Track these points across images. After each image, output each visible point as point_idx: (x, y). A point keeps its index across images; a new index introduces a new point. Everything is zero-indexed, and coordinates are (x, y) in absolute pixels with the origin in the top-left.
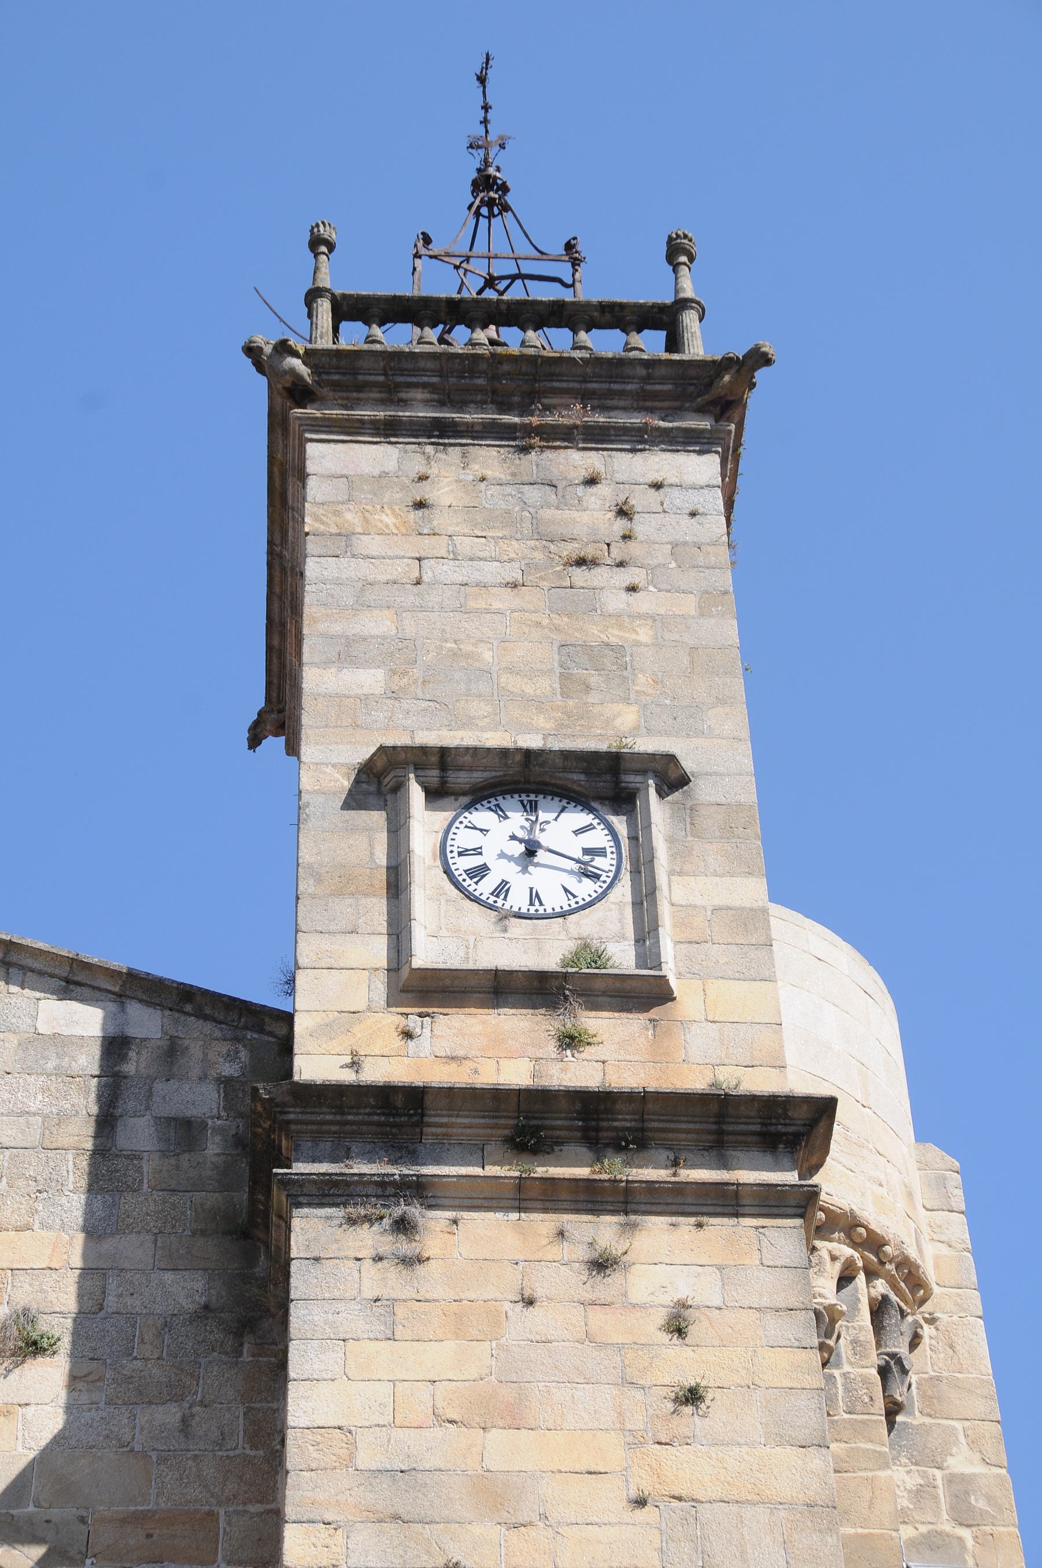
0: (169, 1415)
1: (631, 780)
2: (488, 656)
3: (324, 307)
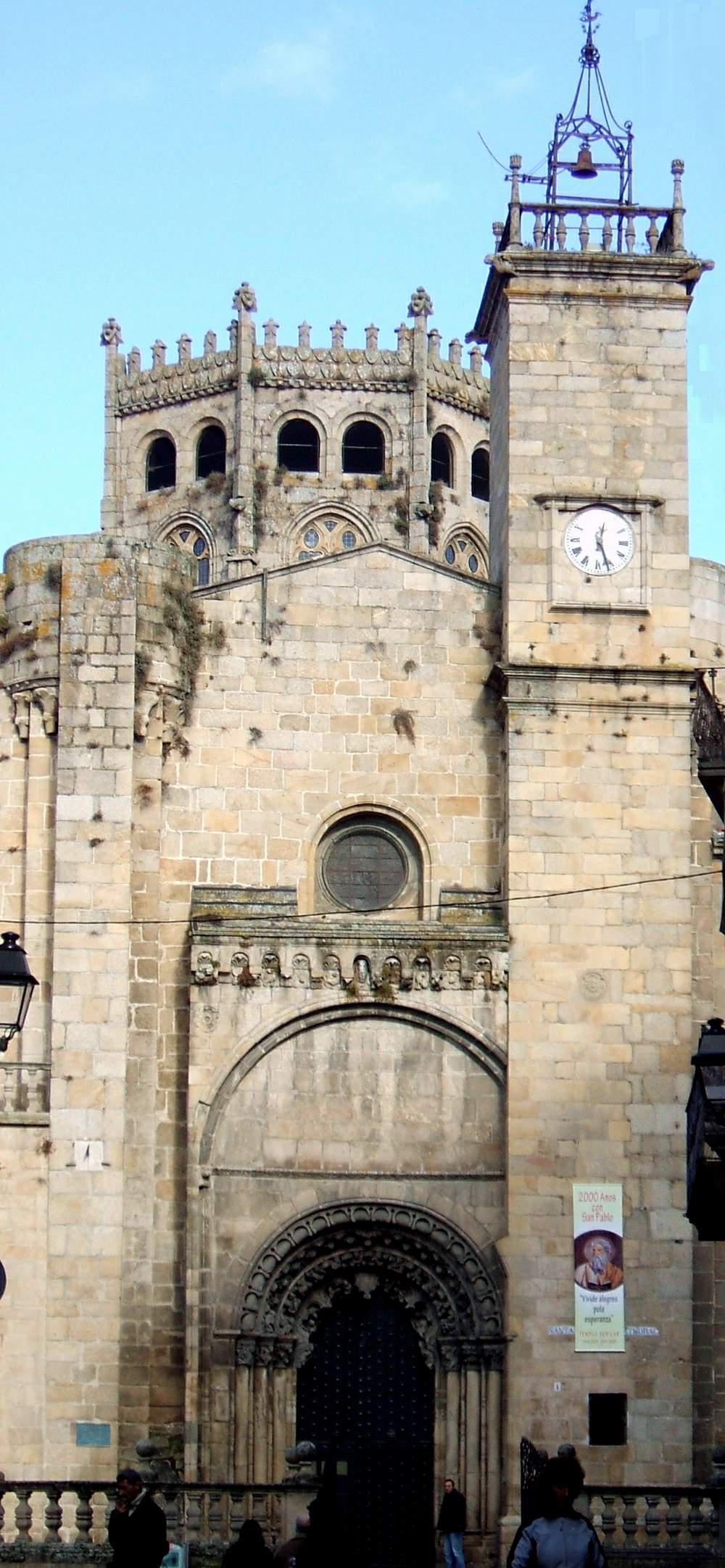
0: (461, 758)
1: (639, 507)
2: (584, 433)
3: (516, 210)
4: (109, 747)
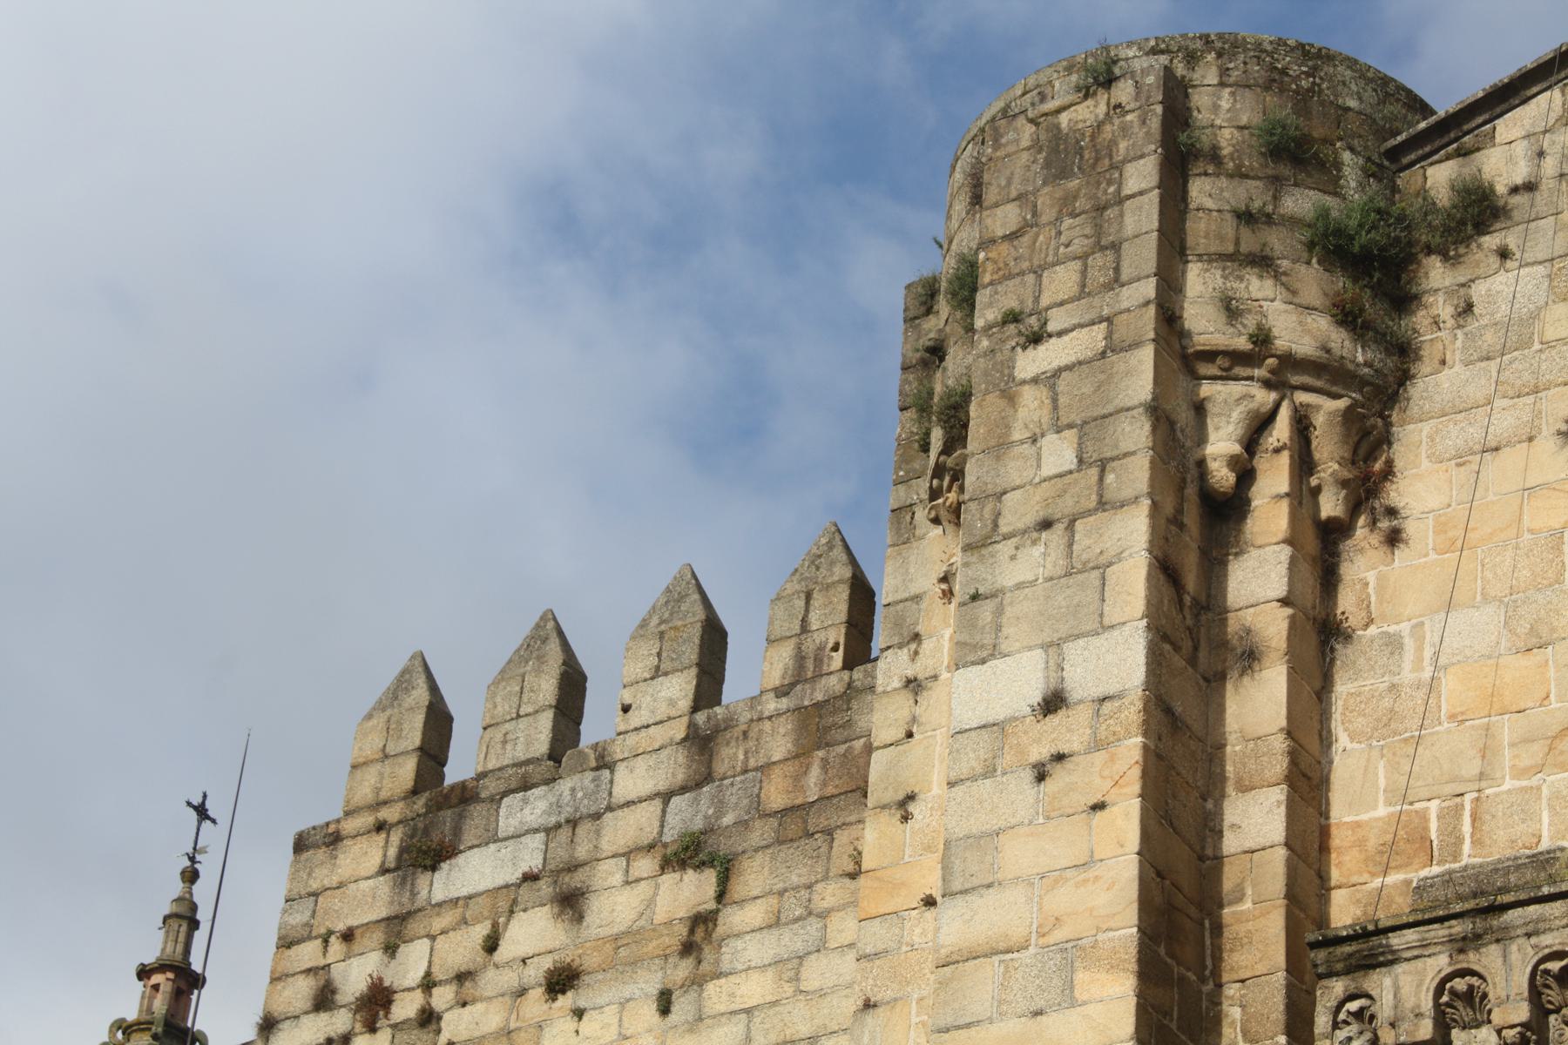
4: (1089, 513)
